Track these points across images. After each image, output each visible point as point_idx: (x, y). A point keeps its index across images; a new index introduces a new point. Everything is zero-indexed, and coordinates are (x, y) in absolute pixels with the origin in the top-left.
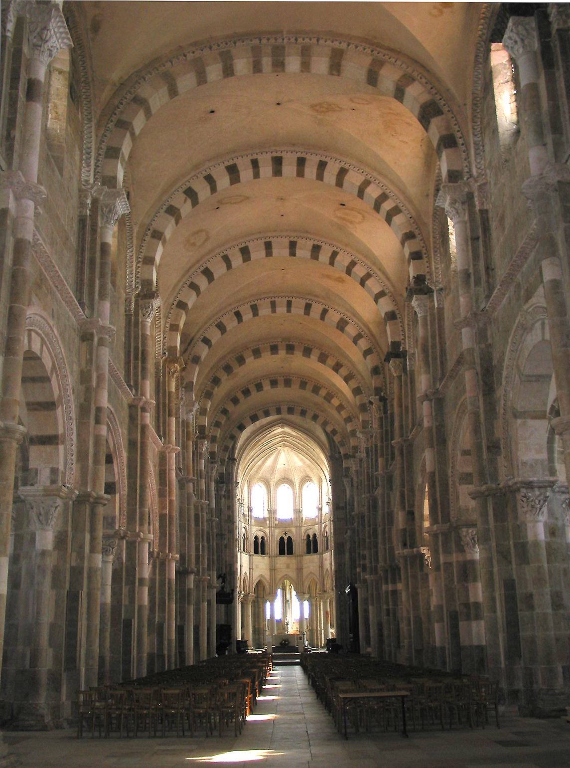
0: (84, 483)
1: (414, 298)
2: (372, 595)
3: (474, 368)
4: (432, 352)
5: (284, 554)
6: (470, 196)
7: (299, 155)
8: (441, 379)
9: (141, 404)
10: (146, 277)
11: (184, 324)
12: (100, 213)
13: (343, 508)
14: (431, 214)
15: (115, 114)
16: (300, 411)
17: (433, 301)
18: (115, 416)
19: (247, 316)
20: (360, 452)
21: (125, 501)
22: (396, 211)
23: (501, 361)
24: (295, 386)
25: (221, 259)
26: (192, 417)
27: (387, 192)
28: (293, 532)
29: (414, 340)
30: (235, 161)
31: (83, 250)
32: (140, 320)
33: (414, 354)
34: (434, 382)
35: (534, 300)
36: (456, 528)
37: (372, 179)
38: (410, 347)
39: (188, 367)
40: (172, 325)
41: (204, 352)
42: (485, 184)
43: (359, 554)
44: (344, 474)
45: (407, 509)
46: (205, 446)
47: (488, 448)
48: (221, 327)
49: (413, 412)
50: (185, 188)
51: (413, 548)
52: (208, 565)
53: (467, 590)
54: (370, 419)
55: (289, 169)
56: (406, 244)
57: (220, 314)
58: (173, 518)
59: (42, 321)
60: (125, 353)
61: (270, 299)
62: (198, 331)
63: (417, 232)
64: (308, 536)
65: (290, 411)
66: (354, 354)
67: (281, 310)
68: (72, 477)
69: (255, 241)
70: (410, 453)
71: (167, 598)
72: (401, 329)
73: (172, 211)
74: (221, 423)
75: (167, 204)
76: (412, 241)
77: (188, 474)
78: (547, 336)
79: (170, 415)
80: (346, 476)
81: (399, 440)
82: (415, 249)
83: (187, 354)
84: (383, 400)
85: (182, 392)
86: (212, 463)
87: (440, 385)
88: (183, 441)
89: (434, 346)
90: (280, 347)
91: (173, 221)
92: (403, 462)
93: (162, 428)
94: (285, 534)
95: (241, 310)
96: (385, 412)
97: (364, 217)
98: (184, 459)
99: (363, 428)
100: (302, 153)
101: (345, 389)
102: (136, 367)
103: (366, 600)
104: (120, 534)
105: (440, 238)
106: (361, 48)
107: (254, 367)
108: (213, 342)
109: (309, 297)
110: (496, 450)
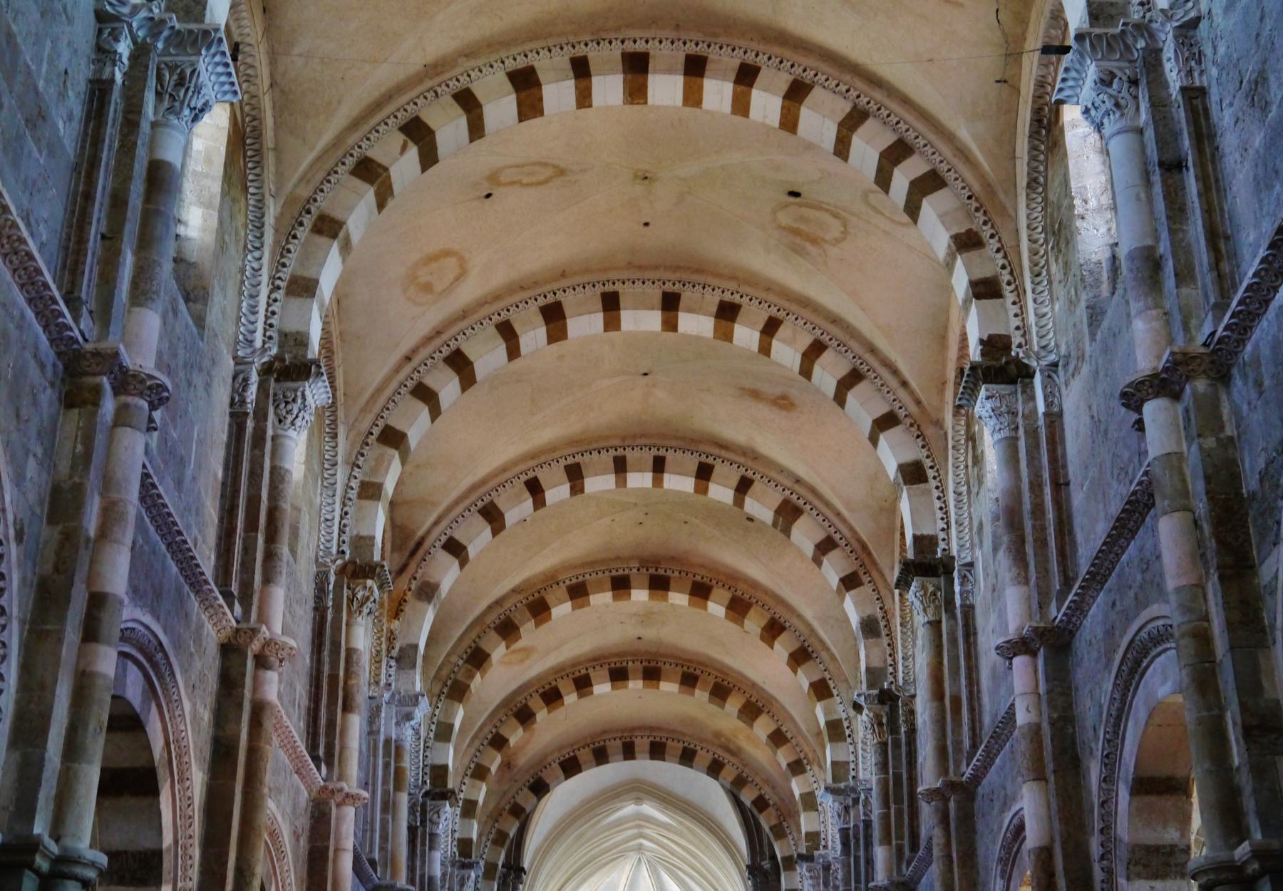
1: (983, 393)
3: (1187, 509)
4: (1034, 527)
6: (1153, 59)
7: (691, 49)
9: (255, 646)
10: (292, 326)
12: (152, 82)
14: (1022, 181)
16: (680, 752)
17: (1032, 398)
18: (173, 659)
19: (558, 492)
20: (825, 847)
22: (929, 183)
24: (669, 687)
25: (492, 330)
26: (408, 733)
27: (912, 134)
29: (971, 529)
30: (534, 60)
31: (94, 163)
32: (270, 432)
33: (971, 565)
37: (872, 105)
41: (447, 574)
42: (1194, 23)
46: (448, 819)
47: (1248, 732)
48: (492, 515)
49: (972, 709)
50: (403, 117)
54: (852, 758)
56: (959, 261)
60: (222, 508)
61: (612, 453)
62: (436, 523)
63: (986, 232)
65: (657, 751)
67: (640, 480)
70: (967, 820)
72: (938, 504)
73: (368, 170)
74: (489, 770)
76: (974, 254)
77: (394, 874)
79: (347, 708)
81: (938, 785)
82: (985, 272)
83: (406, 577)
84: (887, 698)
85: (388, 670)
86: (464, 866)
87: (1058, 612)
88: (386, 793)
89: (1038, 510)
90: (633, 583)
91: (370, 194)
92: (948, 844)
95: (543, 476)
96: (894, 730)
97: (845, 226)
98: (384, 838)
99: (835, 779)
100: (697, 44)
102: (249, 550)
105: (1046, 241)
108: (472, 551)
110: (1273, 736)
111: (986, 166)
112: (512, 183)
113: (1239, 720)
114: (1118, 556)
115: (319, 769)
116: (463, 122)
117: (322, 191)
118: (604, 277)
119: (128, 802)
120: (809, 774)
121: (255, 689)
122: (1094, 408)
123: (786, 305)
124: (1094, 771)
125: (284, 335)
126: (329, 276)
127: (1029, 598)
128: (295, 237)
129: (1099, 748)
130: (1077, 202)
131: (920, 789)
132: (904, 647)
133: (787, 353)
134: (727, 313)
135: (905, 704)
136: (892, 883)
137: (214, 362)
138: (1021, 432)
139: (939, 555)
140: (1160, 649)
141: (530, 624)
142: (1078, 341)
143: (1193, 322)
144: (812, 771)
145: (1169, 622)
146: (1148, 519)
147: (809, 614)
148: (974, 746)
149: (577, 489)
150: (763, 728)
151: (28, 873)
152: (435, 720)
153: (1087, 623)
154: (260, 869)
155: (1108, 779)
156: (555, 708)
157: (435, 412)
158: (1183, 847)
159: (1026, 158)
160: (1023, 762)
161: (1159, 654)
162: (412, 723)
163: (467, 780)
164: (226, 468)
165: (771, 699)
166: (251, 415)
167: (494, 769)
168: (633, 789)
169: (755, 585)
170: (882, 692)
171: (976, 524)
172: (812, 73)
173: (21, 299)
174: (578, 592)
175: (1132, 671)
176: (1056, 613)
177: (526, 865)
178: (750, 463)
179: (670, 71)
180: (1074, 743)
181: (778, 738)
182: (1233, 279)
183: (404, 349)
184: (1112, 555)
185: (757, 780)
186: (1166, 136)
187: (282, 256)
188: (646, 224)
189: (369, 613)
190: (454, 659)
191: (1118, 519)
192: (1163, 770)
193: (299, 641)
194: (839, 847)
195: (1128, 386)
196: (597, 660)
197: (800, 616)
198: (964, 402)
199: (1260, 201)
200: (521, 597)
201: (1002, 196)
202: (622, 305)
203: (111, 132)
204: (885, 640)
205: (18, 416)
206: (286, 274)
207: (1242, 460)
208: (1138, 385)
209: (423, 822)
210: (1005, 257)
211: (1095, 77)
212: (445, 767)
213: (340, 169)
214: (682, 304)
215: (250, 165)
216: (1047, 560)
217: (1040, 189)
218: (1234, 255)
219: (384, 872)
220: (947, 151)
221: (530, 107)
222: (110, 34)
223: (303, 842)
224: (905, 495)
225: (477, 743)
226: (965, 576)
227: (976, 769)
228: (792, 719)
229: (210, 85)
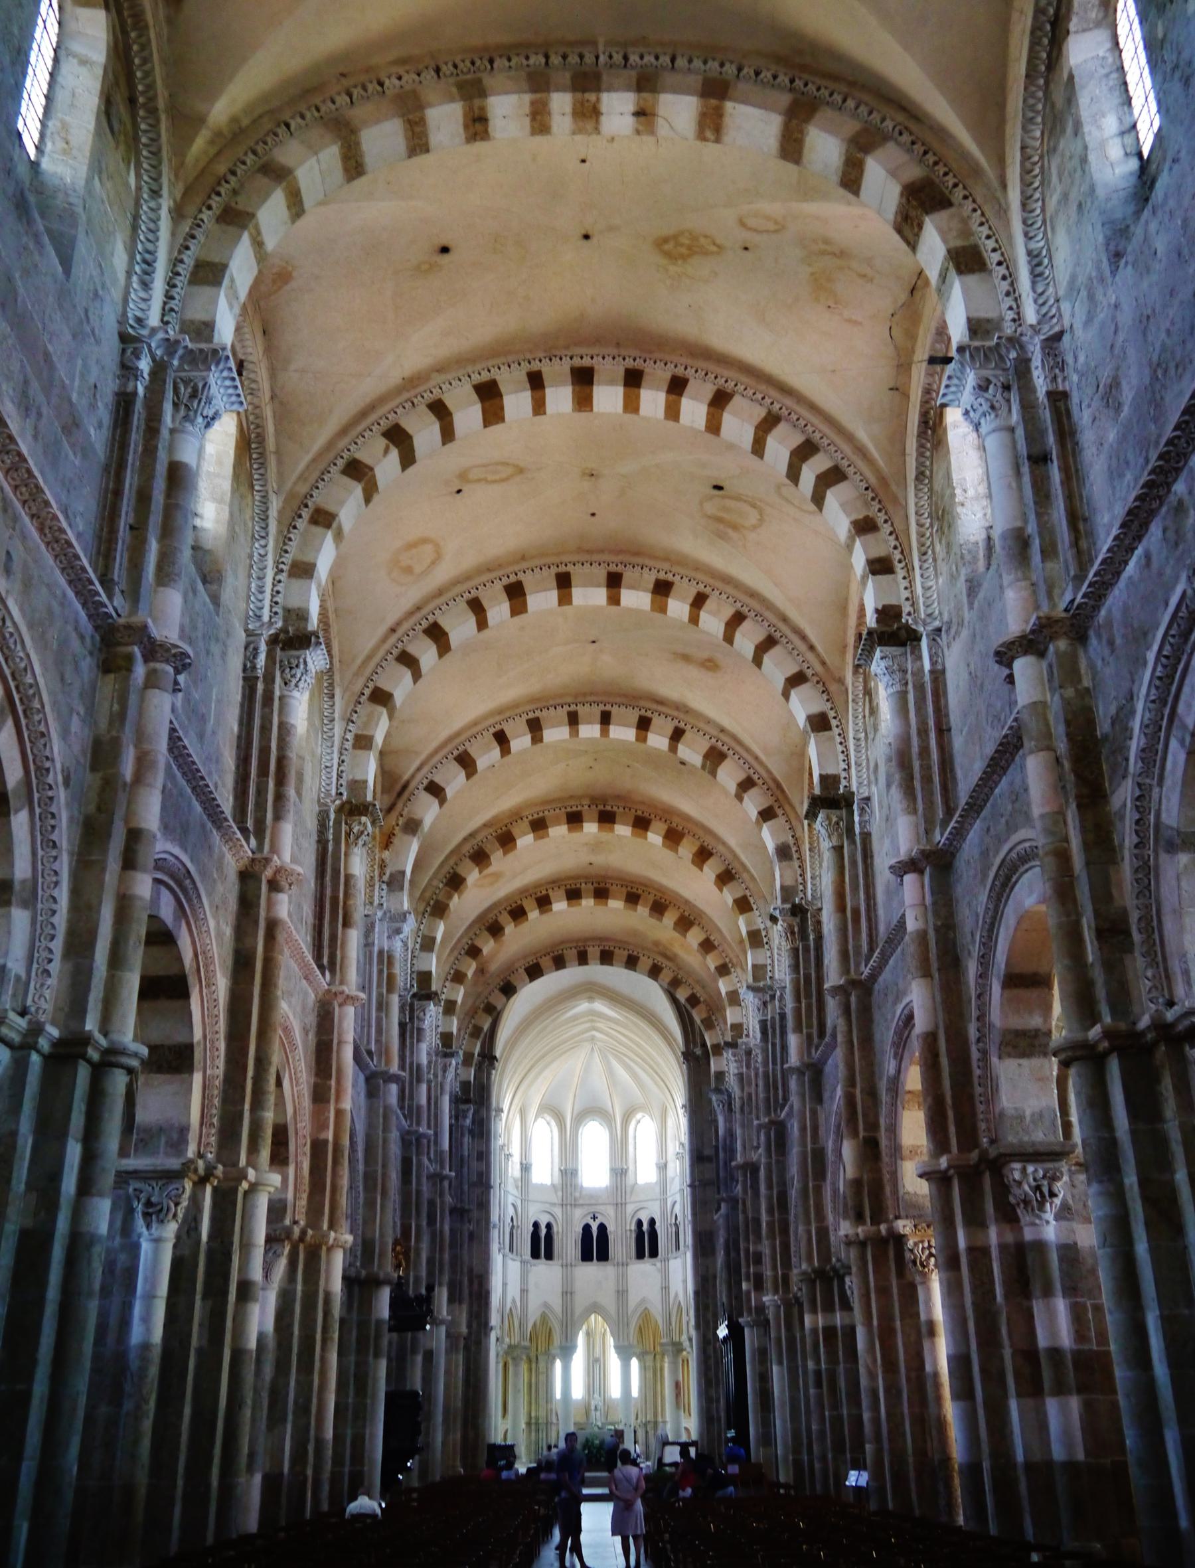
0: (76, 1005)
1: (878, 653)
2: (779, 1340)
3: (1050, 748)
4: (921, 766)
5: (591, 1259)
7: (630, 363)
8: (945, 823)
9: (268, 873)
10: (294, 603)
12: (170, 394)
13: (709, 1159)
14: (911, 474)
15: (218, 194)
16: (625, 959)
17: (920, 658)
18: (199, 884)
19: (521, 742)
20: (747, 1036)
21: (216, 1092)
22: (832, 477)
23: (1122, 719)
25: (465, 606)
26: (398, 945)
27: (817, 435)
28: (609, 1218)
29: (868, 769)
30: (495, 374)
31: (121, 465)
32: (277, 693)
33: (868, 799)
34: (927, 832)
36: (997, 1165)
37: (784, 412)
38: (860, 784)
39: (396, 841)
40: (358, 738)
41: (428, 811)
43: (747, 1250)
44: (713, 1085)
45: (861, 1134)
46: (432, 1015)
47: (1100, 934)
48: (466, 762)
49: (869, 919)
51: (879, 1224)
52: (430, 1273)
53: (1029, 1318)
56: (858, 544)
57: (462, 738)
58: (342, 1152)
60: (238, 758)
62: (419, 769)
63: (881, 518)
64: (640, 1223)
65: (607, 958)
67: (590, 731)
68: (47, 993)
69: (537, 570)
71: (319, 1336)
73: (356, 470)
74: (466, 975)
75: (346, 455)
76: (869, 537)
77: (388, 1062)
79: (347, 924)
80: (718, 1090)
81: (842, 982)
82: (879, 551)
83: (394, 814)
84: (798, 911)
85: (380, 892)
86: (446, 1055)
87: (942, 835)
88: (380, 995)
89: (924, 752)
90: (585, 816)
91: (358, 490)
92: (850, 1031)
93: (326, 952)
94: (594, 1218)
95: (509, 729)
96: (804, 936)
97: (761, 515)
99: (755, 978)
100: (635, 360)
102: (261, 792)
103: (762, 1354)
104: (196, 1170)
105: (931, 526)
106: (769, 75)
108: (449, 792)
111: (881, 463)
112: (479, 480)
113: (1093, 925)
114: (992, 789)
115: (323, 975)
116: (436, 428)
117: (317, 488)
118: (556, 560)
119: (164, 1004)
120: (733, 976)
122: (972, 666)
123: (711, 581)
124: (972, 968)
125: (288, 611)
126: (325, 560)
127: (917, 826)
128: (295, 527)
129: (975, 950)
130: (958, 491)
131: (826, 986)
132: (812, 868)
133: (712, 622)
134: (662, 589)
135: (813, 916)
136: (803, 1064)
137: (228, 634)
138: (910, 686)
139: (841, 791)
140: (1027, 866)
141: (500, 852)
142: (958, 609)
143: (1056, 591)
144: (736, 973)
145: (1034, 844)
146: (1017, 758)
147: (732, 842)
148: (871, 950)
149: (537, 738)
150: (694, 937)
151: (82, 1063)
152: (420, 934)
153: (966, 846)
154: (276, 1058)
155: (983, 976)
156: (520, 923)
157: (417, 675)
158: (1044, 1029)
159: (914, 455)
160: (912, 963)
161: (1027, 871)
162: (401, 936)
163: (447, 984)
164: (241, 724)
165: (701, 914)
166: (261, 679)
167: (470, 974)
168: (587, 990)
169: (687, 818)
170: (794, 906)
171: (872, 765)
172: (733, 384)
173: (62, 581)
174: (539, 826)
175: (1004, 885)
176: (940, 838)
177: (498, 1054)
178: (681, 716)
179: (612, 382)
180: (954, 945)
181: (707, 946)
182: (1090, 554)
183: (390, 621)
184: (986, 790)
185: (690, 981)
186: (1033, 433)
187: (285, 544)
188: (593, 515)
189: (364, 845)
191: (992, 759)
192: (1027, 968)
193: (305, 868)
194: (759, 1035)
195: (1001, 646)
196: (555, 882)
197: (724, 844)
198: (862, 662)
199: (1114, 488)
200: (491, 830)
201: (894, 487)
202: (573, 583)
203: (136, 437)
204: (796, 863)
205: (62, 679)
206: (288, 559)
207: (1097, 707)
208: (1010, 645)
209: (411, 1019)
210: (897, 539)
211: (974, 383)
212: (430, 973)
213: (333, 469)
215: (255, 466)
216: (932, 793)
217: (927, 481)
218: (1091, 534)
219: (379, 1060)
220: (847, 449)
221: (493, 414)
222: (132, 353)
223: (311, 1036)
224: (812, 741)
225: (456, 953)
226: (863, 809)
227: (873, 969)
229: (219, 396)
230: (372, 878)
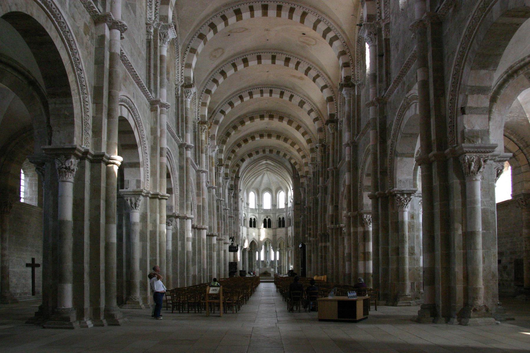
8: (357, 135)
10: (187, 75)
11: (210, 102)
19: (247, 99)
23: (391, 125)
25: (230, 65)
30: (240, 7)
32: (184, 100)
33: (342, 121)
35: (412, 92)
38: (340, 117)
39: (212, 126)
48: (231, 104)
49: (340, 152)
55: (272, 13)
59: (128, 99)
66: (308, 121)
67: (266, 95)
74: (231, 158)
78: (418, 112)
79: (202, 153)
83: (211, 119)
84: (323, 146)
85: (209, 141)
89: (354, 116)
90: (265, 116)
96: (325, 152)
99: (312, 161)
101: (303, 140)
102: (182, 126)
107: (250, 127)
108: (227, 113)
109: (283, 88)
116: (223, 23)
121: (186, 155)
127: (350, 135)
150: (297, 147)
164: (176, 109)
169: (295, 117)
181: (299, 150)
190: (223, 135)
196: (256, 132)
204: (324, 133)
214: (277, 58)
225: (228, 152)
228: (303, 146)
230: (206, 137)
